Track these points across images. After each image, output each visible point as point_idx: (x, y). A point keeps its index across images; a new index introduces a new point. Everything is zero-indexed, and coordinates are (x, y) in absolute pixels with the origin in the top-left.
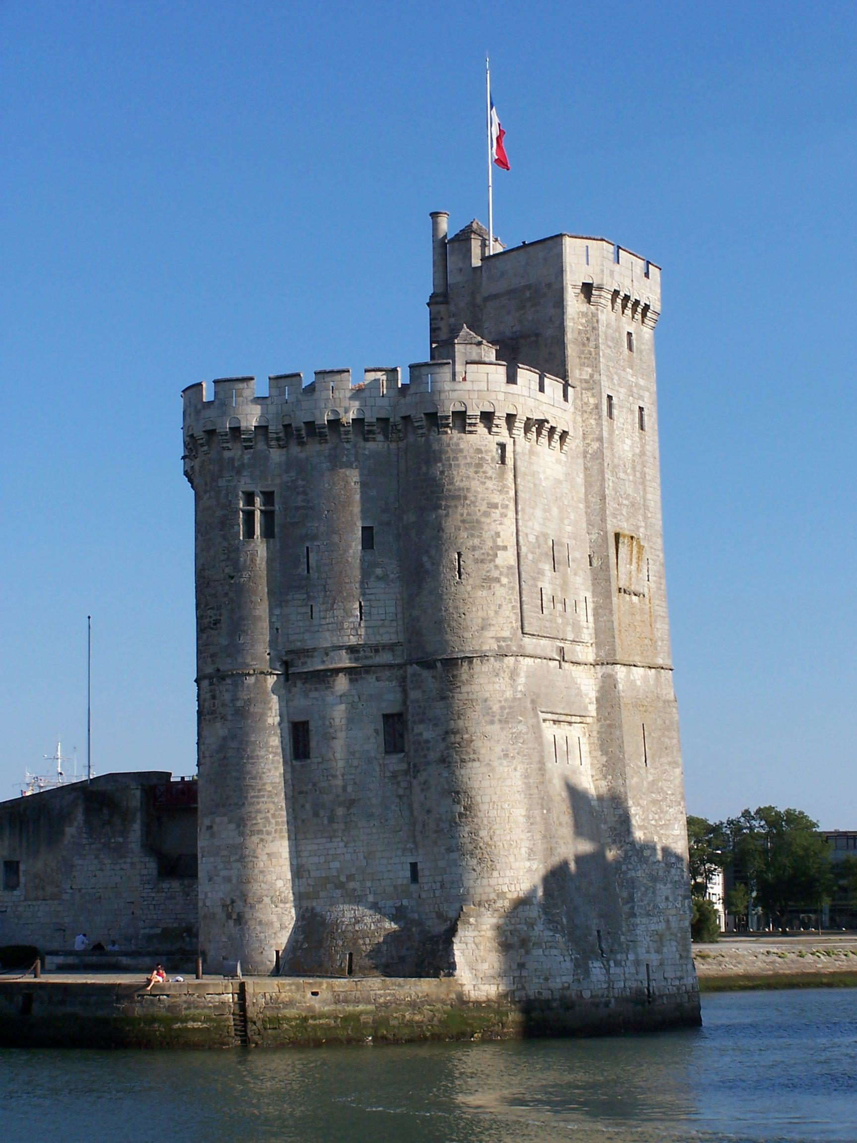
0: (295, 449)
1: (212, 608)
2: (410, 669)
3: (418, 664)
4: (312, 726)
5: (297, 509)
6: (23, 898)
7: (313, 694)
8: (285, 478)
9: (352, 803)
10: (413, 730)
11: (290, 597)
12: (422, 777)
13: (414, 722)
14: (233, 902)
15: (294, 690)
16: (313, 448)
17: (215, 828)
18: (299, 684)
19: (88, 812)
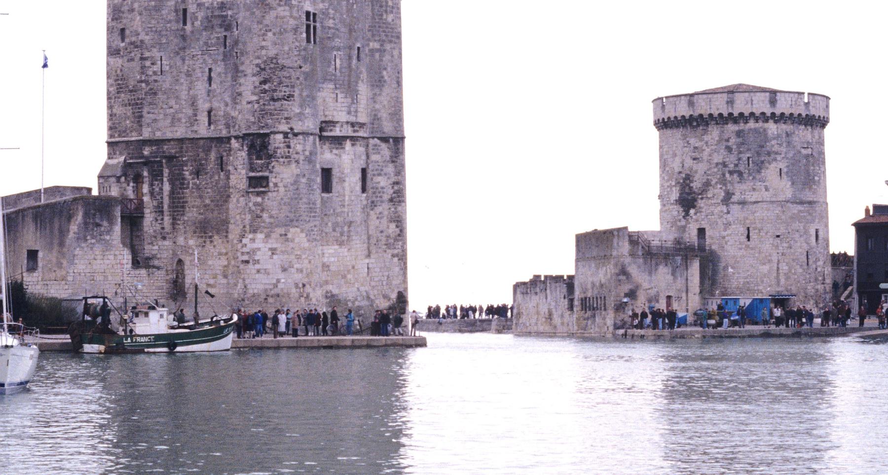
1: (287, 86)
2: (371, 141)
3: (379, 138)
4: (335, 172)
5: (329, 28)
6: (40, 279)
7: (335, 151)
8: (321, 6)
9: (351, 222)
10: (372, 179)
11: (324, 86)
12: (379, 209)
13: (374, 175)
14: (304, 285)
15: (324, 147)
17: (290, 236)
18: (327, 144)
19: (86, 215)
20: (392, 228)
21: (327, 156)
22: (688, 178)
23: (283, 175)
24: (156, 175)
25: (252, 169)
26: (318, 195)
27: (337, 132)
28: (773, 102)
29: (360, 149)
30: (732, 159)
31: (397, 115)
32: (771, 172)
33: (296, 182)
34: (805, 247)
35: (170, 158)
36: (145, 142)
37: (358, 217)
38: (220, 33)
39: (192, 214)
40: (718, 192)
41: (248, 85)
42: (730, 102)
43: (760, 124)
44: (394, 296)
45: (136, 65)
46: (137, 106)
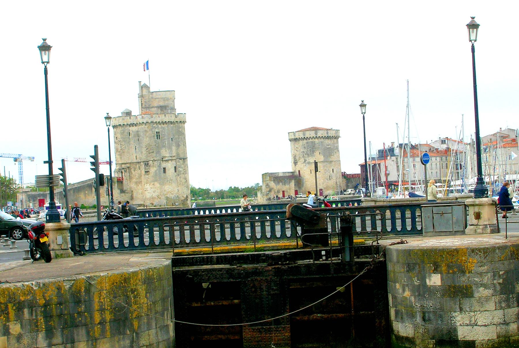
0: (162, 125)
16: (165, 125)
20: (184, 181)
21: (164, 165)
22: (295, 156)
23: (153, 170)
24: (125, 171)
25: (145, 169)
26: (163, 175)
27: (167, 159)
28: (316, 134)
29: (174, 162)
30: (305, 150)
31: (185, 152)
32: (317, 153)
33: (156, 171)
34: (329, 174)
35: (128, 167)
36: (122, 164)
37: (174, 178)
38: (137, 138)
39: (134, 180)
40: (302, 160)
41: (144, 150)
42: (304, 134)
43: (313, 140)
44: (185, 196)
45: (120, 146)
46: (120, 155)
